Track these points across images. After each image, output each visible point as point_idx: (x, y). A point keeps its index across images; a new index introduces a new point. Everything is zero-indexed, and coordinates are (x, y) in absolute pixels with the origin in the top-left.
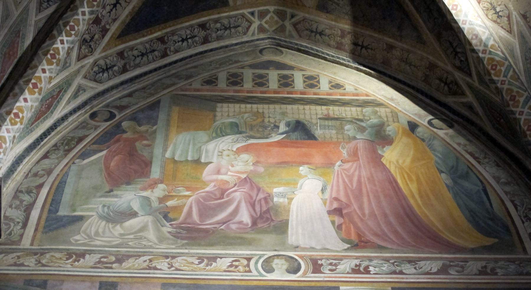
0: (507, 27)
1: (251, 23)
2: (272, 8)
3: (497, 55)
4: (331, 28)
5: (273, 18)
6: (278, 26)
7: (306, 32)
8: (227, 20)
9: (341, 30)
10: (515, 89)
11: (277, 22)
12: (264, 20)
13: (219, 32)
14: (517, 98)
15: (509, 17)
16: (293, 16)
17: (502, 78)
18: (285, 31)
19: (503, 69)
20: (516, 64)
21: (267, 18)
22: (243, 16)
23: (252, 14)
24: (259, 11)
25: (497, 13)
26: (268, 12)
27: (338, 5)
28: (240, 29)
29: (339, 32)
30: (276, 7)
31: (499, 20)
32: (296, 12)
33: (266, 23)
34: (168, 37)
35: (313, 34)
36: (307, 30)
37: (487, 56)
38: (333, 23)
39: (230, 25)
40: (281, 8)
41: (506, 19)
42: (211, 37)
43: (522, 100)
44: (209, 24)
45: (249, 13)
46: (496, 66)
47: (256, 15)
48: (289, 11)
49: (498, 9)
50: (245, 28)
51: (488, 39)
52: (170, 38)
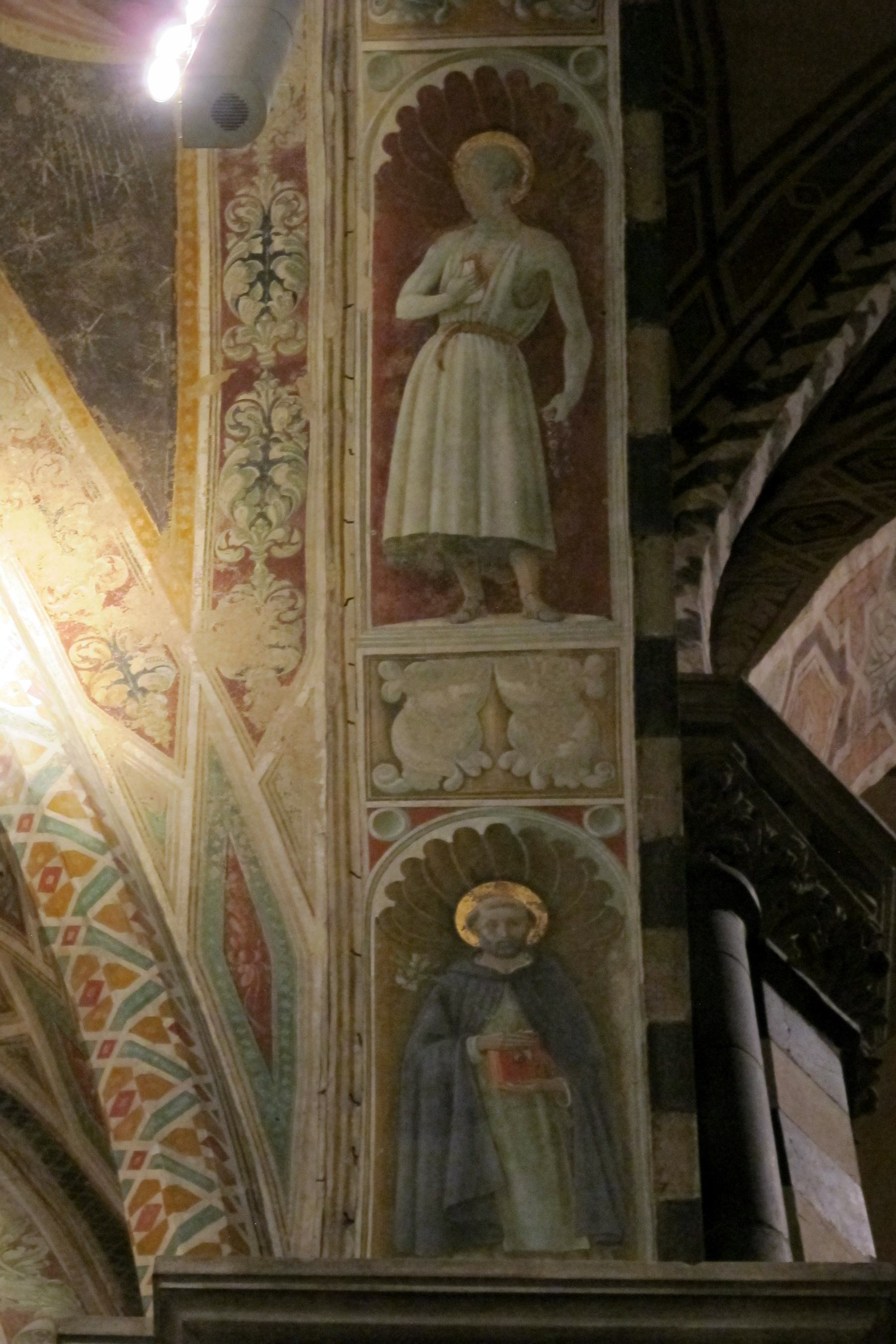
0: (157, 726)
3: (71, 833)
10: (105, 958)
14: (105, 992)
15: (173, 694)
17: (69, 919)
19: (78, 884)
20: (161, 869)
25: (130, 678)
31: (131, 707)
37: (34, 838)
41: (163, 699)
43: (119, 996)
46: (56, 872)
49: (136, 667)
51: (49, 773)
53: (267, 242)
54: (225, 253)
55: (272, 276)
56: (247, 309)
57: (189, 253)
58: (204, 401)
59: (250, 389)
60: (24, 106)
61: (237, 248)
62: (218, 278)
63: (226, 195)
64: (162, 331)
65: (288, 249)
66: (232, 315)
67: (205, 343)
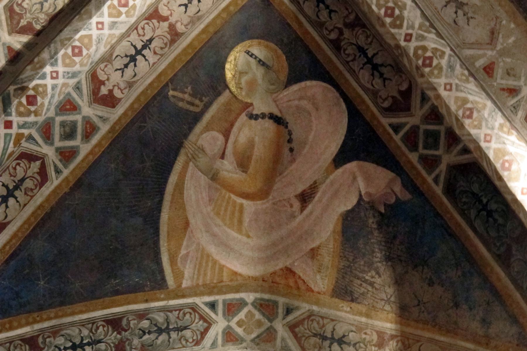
1: (209, 324)
2: (250, 297)
4: (360, 329)
5: (253, 315)
6: (262, 329)
7: (313, 340)
8: (162, 314)
9: (377, 332)
11: (259, 324)
12: (236, 319)
13: (147, 336)
16: (288, 311)
18: (275, 339)
21: (242, 315)
22: (194, 308)
23: (213, 306)
24: (224, 301)
26: (242, 303)
27: (372, 284)
28: (188, 333)
29: (375, 337)
30: (258, 295)
32: (296, 303)
33: (240, 324)
34: (44, 339)
35: (327, 343)
36: (315, 335)
38: (363, 319)
39: (168, 325)
40: (266, 296)
42: (130, 345)
44: (128, 319)
45: (206, 304)
47: (220, 308)
48: (281, 300)
50: (198, 333)
52: (48, 340)
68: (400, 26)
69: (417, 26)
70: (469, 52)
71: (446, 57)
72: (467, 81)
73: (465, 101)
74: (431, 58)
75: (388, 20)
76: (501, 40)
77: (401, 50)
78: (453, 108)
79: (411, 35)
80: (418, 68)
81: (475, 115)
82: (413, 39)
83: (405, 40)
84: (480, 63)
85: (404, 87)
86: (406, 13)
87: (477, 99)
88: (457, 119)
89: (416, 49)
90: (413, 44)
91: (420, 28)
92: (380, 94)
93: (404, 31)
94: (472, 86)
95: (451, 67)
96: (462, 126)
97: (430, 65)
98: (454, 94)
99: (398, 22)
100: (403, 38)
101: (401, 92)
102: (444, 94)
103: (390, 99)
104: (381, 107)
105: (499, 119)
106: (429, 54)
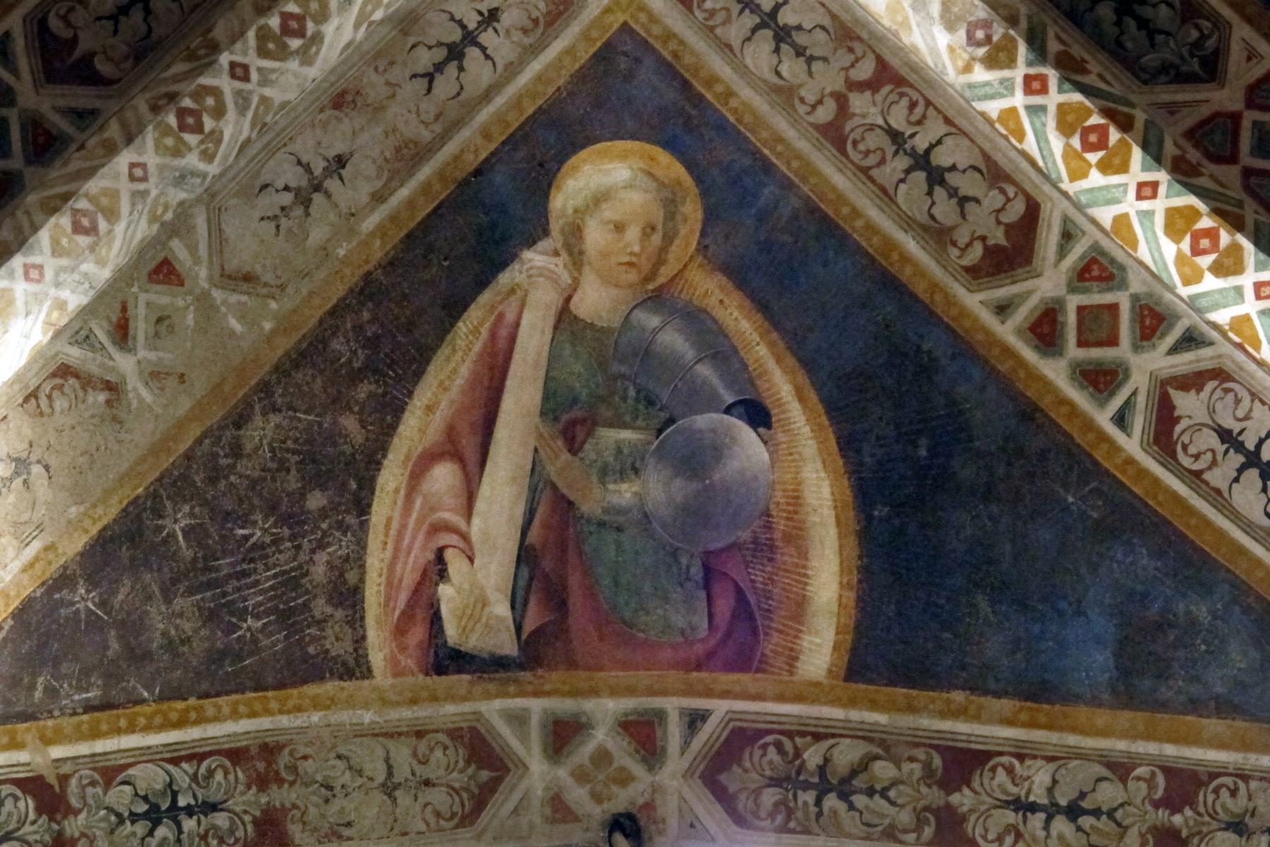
53: (190, 811)
54: (175, 761)
55: (156, 823)
56: (120, 797)
57: (174, 716)
58: (23, 756)
59: (39, 811)
60: (316, 501)
61: (182, 775)
62: (147, 756)
63: (236, 755)
64: (93, 694)
65: (184, 837)
66: (114, 778)
67: (83, 749)
68: (263, 52)
69: (267, 92)
70: (200, 221)
71: (202, 166)
72: (153, 218)
73: (112, 215)
74: (199, 128)
75: (274, 22)
76: (234, 298)
77: (206, 55)
78: (94, 185)
79: (246, 78)
80: (172, 97)
81: (83, 240)
82: (238, 85)
83: (233, 65)
84: (178, 249)
85: (103, 67)
86: (293, 64)
87: (117, 244)
88: (66, 197)
89: (216, 92)
90: (227, 85)
91: (264, 100)
92: (78, 7)
93: (256, 63)
94: (143, 229)
95: (181, 178)
96: (51, 208)
97: (183, 127)
98: (125, 187)
99: (271, 46)
100: (238, 58)
101: (88, 58)
102: (124, 160)
103: (67, 34)
104: (49, 12)
105: (75, 299)
106: (208, 123)
